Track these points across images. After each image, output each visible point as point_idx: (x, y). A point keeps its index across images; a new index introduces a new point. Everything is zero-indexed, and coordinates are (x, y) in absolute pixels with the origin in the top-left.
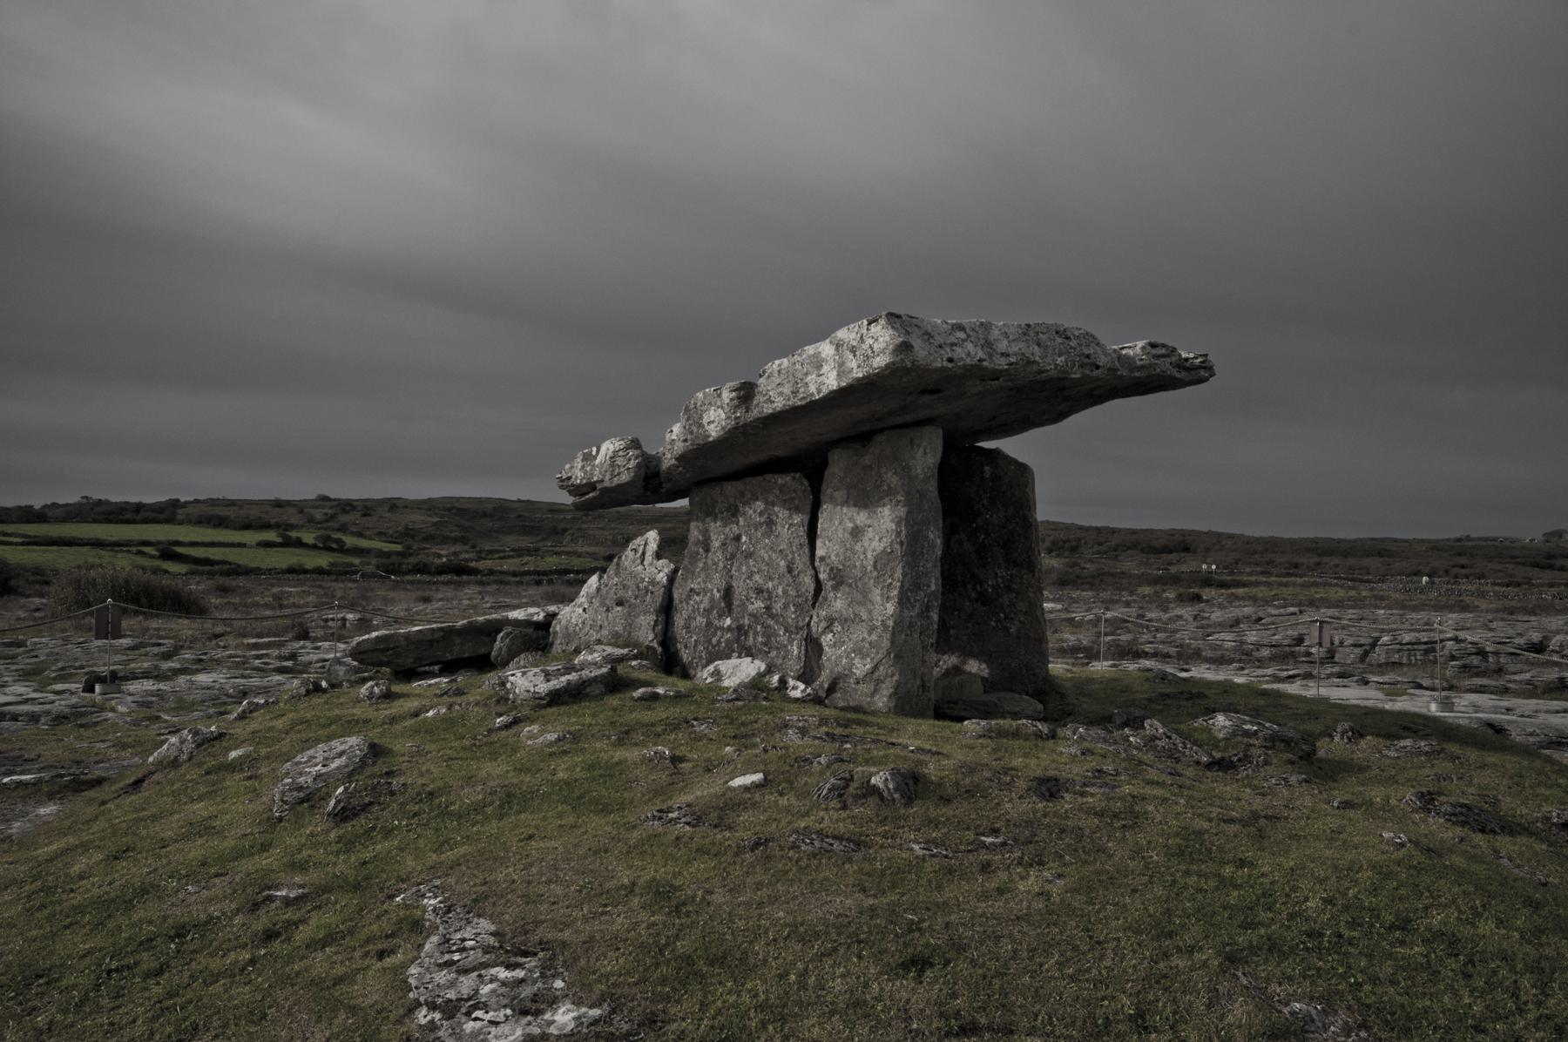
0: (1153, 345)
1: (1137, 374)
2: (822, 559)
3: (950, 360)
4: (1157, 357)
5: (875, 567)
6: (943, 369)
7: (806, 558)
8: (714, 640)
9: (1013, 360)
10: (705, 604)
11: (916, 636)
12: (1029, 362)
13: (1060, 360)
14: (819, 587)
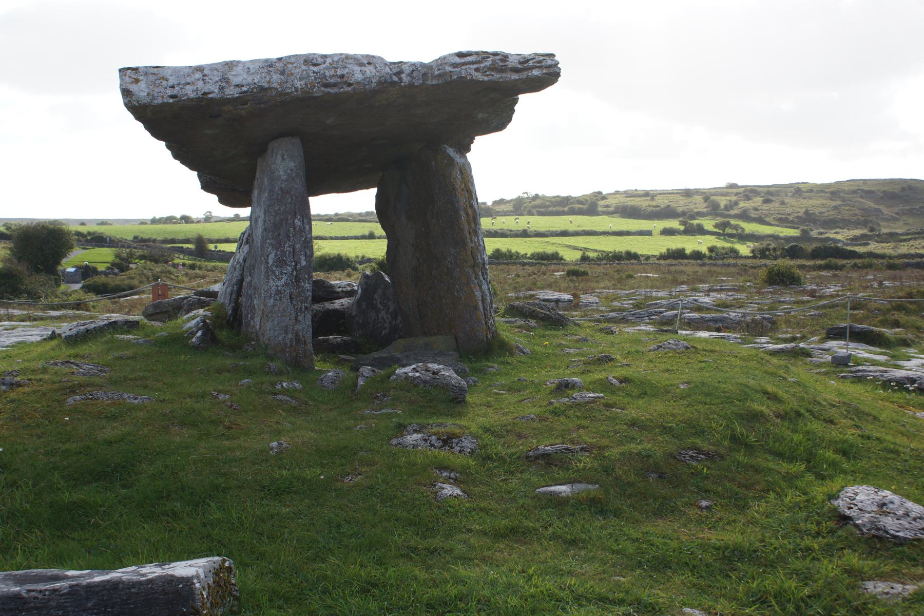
0: (460, 55)
1: (434, 82)
3: (172, 97)
4: (455, 65)
6: (164, 104)
9: (244, 89)
11: (286, 301)
12: (262, 89)
13: (298, 84)
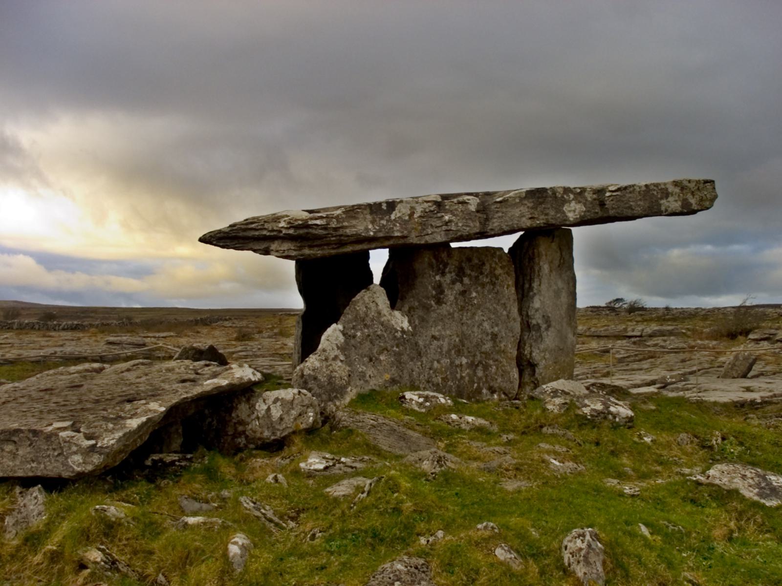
2: (537, 310)
7: (515, 310)
8: (458, 376)
14: (527, 326)
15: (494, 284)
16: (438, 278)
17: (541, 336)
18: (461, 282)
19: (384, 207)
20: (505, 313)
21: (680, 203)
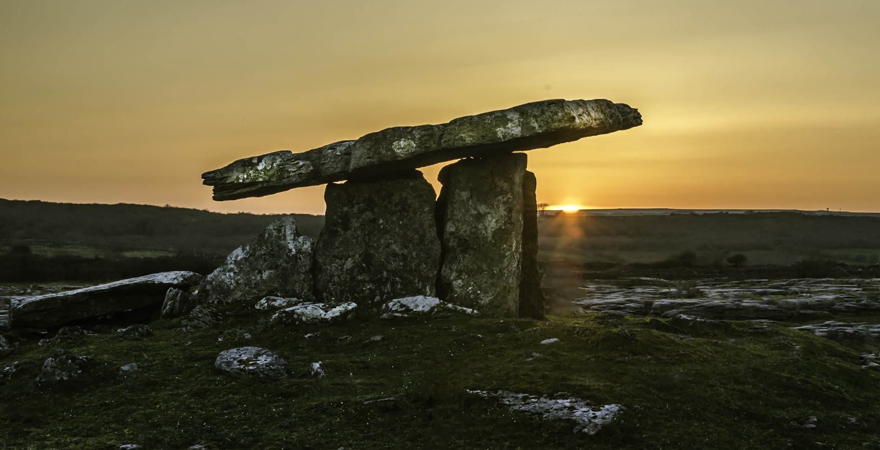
2: (452, 233)
5: (493, 237)
8: (358, 290)
10: (349, 264)
14: (445, 250)
15: (407, 211)
16: (346, 209)
17: (456, 258)
18: (372, 211)
19: (255, 161)
20: (416, 237)
21: (520, 128)
